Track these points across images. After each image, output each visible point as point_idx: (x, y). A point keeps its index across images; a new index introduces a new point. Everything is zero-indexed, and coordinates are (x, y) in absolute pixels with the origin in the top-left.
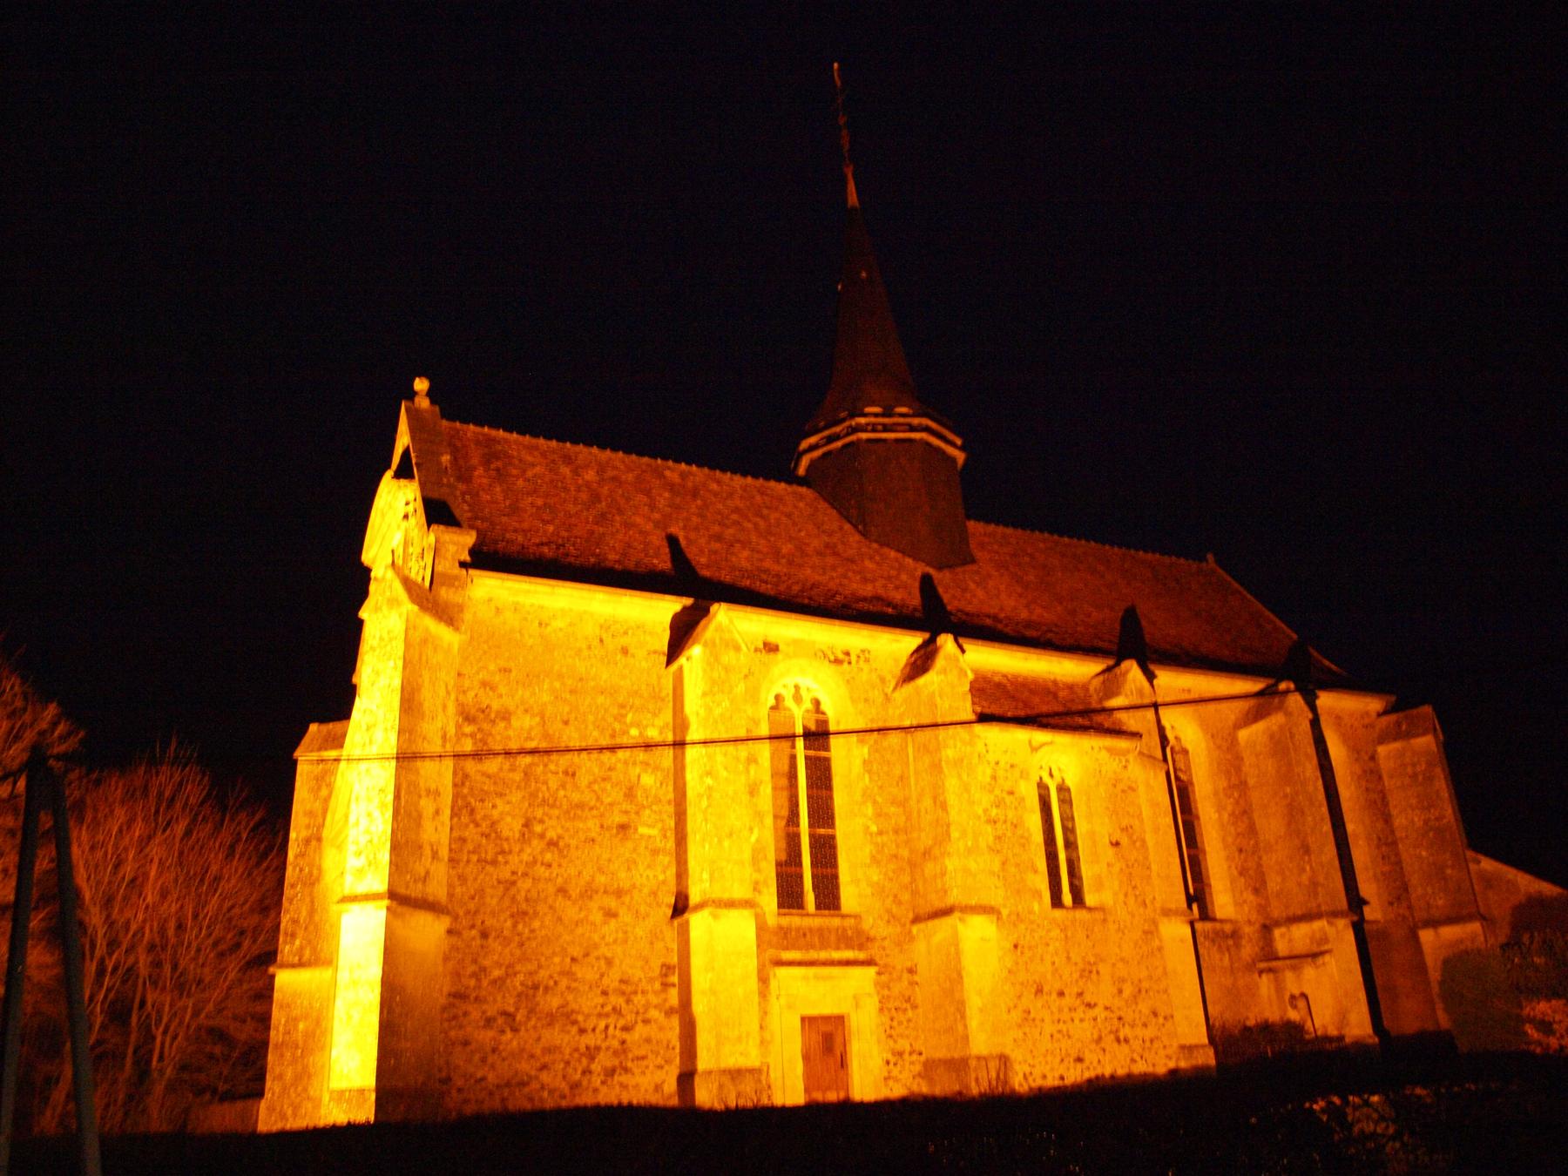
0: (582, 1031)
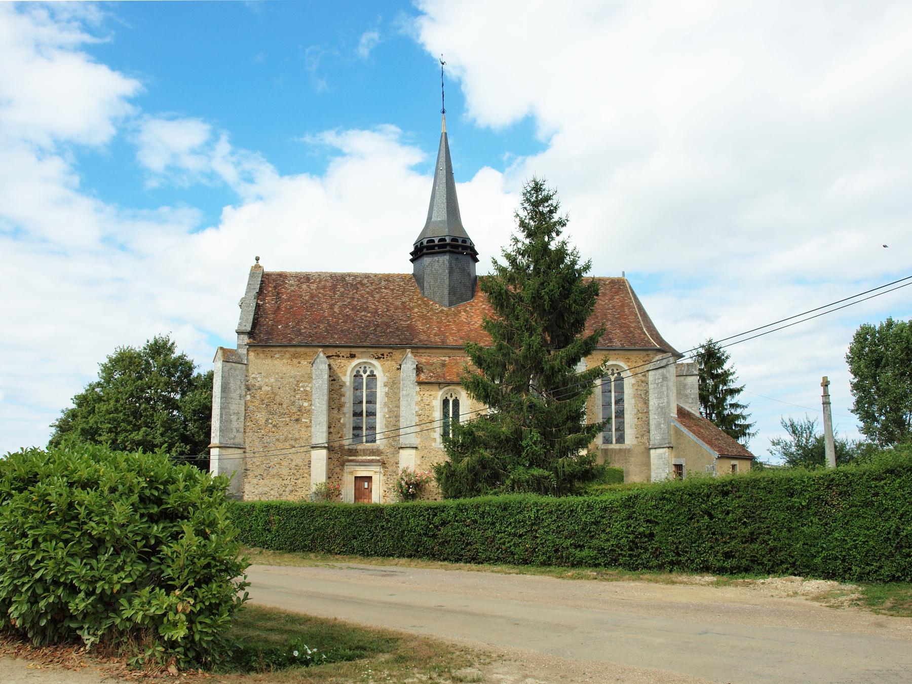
0: (283, 480)
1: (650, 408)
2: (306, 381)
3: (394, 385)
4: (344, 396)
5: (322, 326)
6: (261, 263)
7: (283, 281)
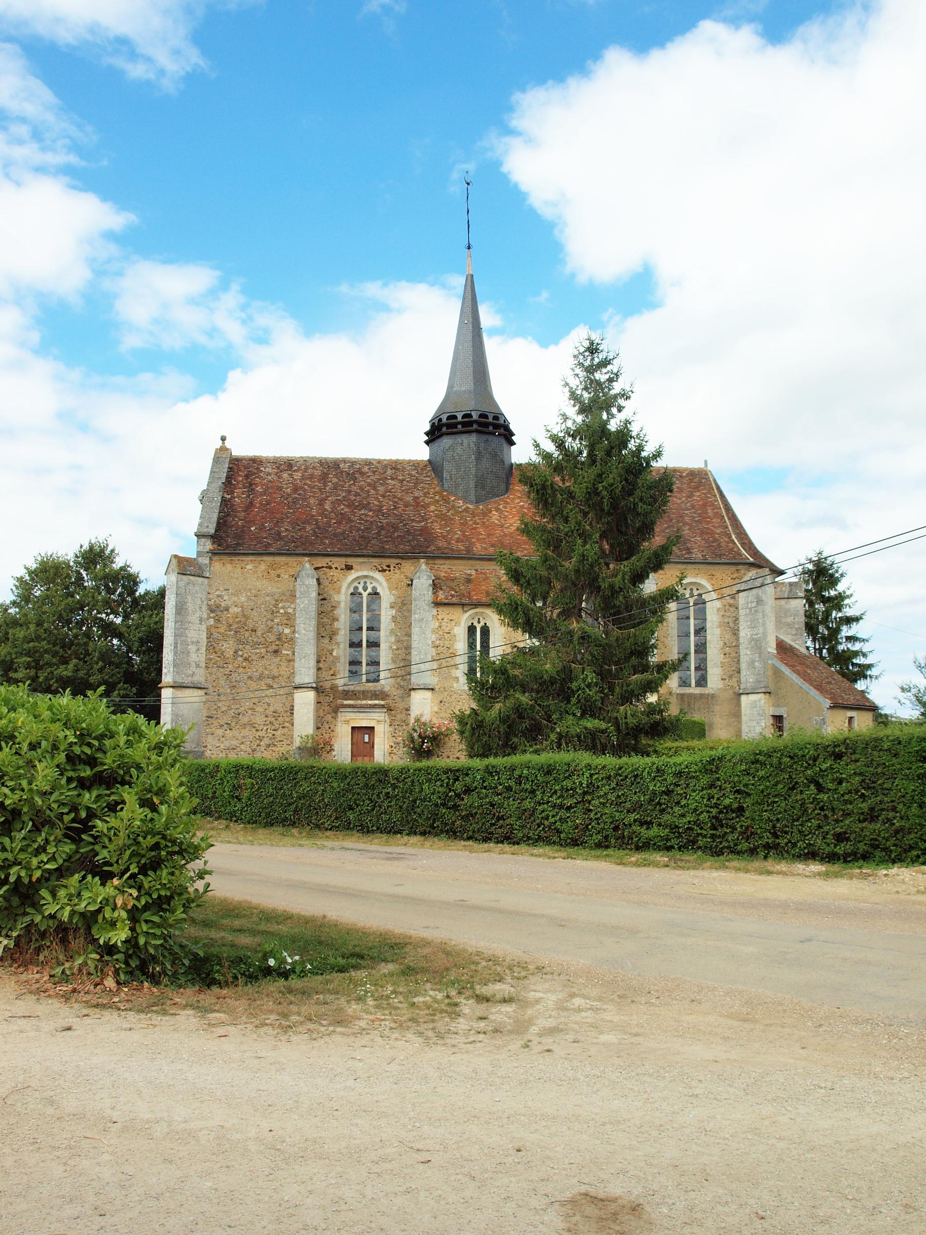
0: (257, 730)
1: (741, 641)
2: (287, 601)
3: (404, 607)
4: (337, 620)
5: (308, 528)
6: (228, 444)
7: (258, 468)
